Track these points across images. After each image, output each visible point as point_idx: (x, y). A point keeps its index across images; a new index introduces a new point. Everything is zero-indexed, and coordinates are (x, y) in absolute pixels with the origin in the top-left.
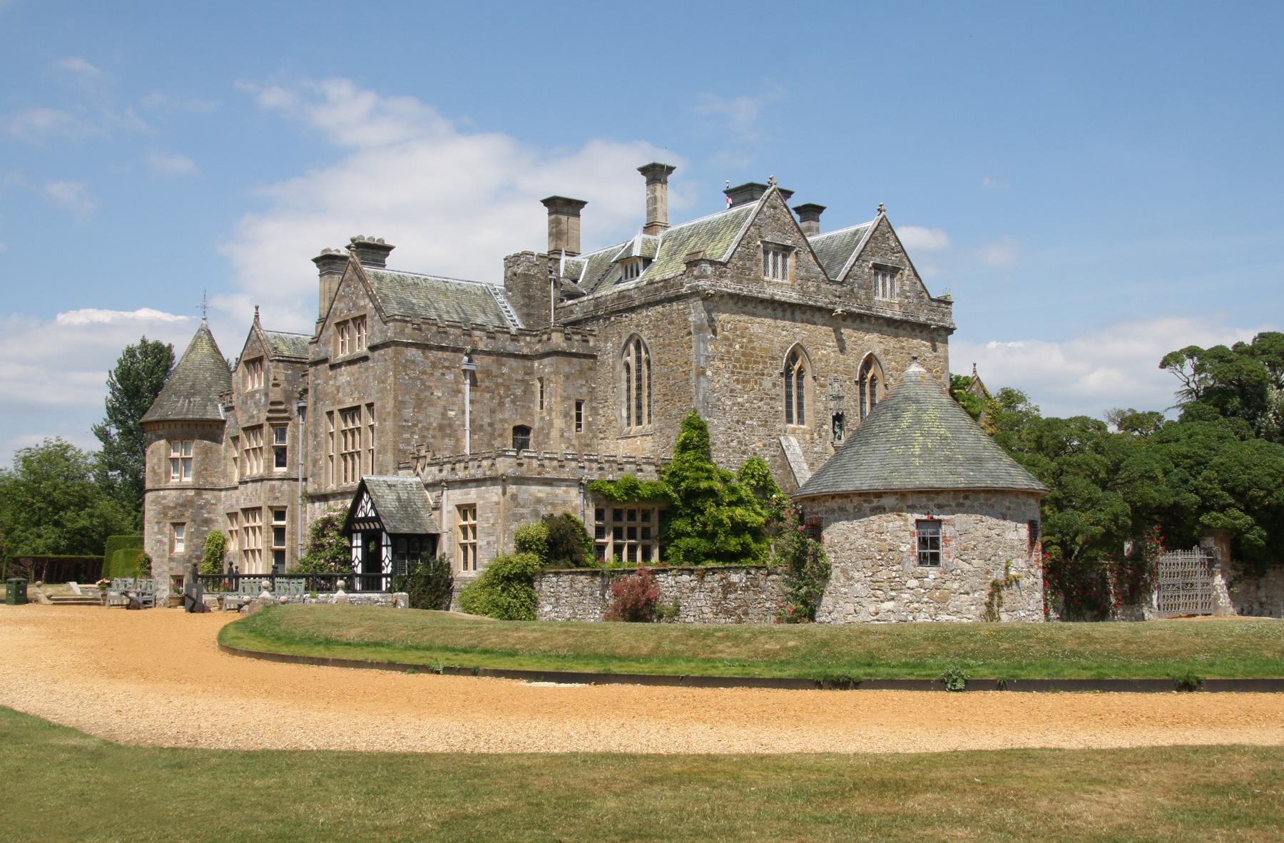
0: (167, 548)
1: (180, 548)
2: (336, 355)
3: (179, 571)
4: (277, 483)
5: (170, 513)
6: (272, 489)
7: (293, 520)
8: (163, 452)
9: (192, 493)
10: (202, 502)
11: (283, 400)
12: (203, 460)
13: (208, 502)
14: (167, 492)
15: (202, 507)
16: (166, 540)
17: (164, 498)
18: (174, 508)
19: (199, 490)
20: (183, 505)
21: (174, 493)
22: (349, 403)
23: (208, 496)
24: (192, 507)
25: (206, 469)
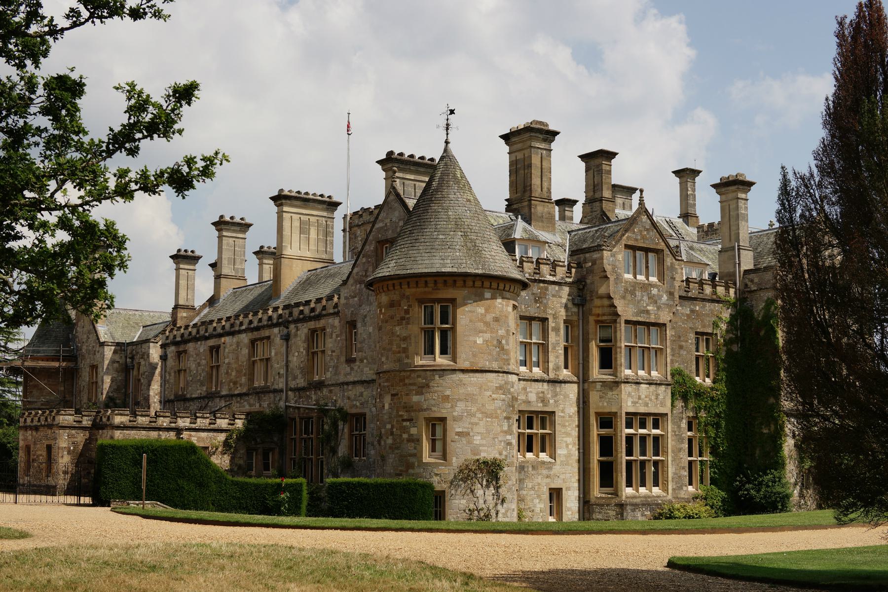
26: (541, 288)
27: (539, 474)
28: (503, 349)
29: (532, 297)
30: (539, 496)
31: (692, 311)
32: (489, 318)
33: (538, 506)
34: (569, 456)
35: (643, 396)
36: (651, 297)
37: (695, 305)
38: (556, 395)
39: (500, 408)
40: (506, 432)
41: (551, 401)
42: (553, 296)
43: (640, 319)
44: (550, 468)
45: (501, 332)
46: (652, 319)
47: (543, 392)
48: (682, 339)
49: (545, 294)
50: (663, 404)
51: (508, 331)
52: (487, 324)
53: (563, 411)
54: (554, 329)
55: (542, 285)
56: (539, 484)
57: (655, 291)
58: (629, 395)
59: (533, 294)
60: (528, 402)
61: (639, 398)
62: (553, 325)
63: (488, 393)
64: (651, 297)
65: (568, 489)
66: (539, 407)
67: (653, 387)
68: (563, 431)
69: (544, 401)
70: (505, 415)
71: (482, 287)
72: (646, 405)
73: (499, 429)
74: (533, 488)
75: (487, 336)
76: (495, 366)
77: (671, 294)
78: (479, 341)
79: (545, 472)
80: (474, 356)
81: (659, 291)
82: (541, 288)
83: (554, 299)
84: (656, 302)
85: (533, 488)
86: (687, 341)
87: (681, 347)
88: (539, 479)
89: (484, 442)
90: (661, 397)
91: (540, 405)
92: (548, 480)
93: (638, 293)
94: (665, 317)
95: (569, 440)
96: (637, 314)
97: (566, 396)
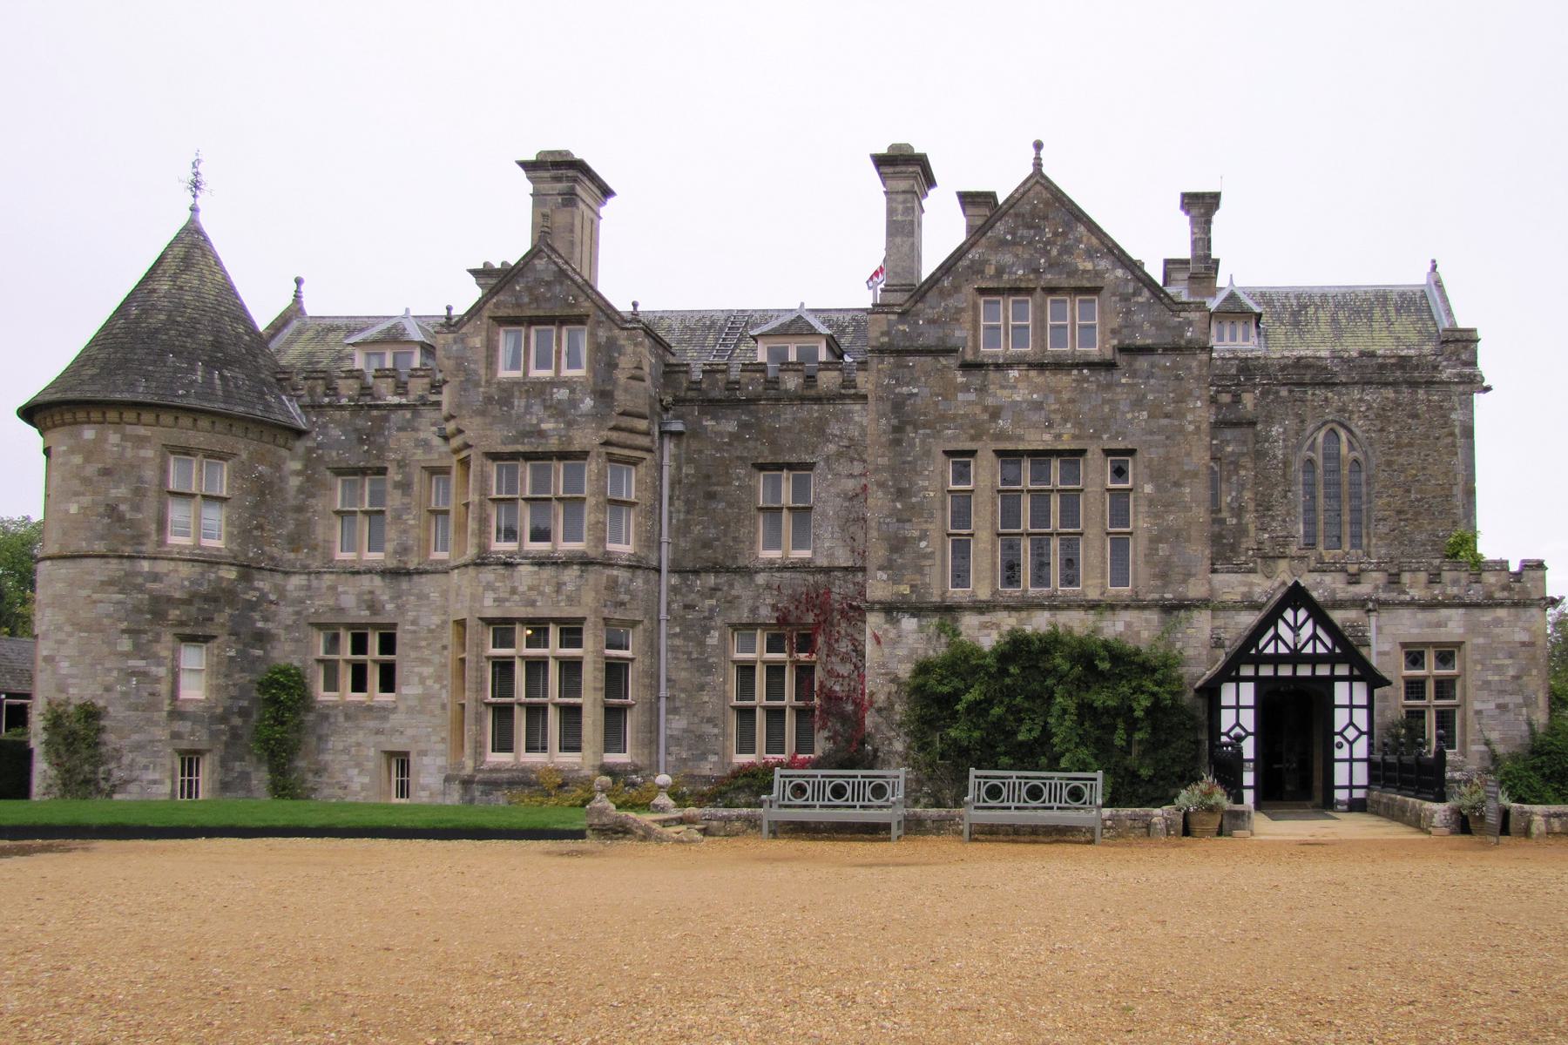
3: (198, 737)
5: (174, 614)
6: (613, 585)
7: (653, 649)
8: (150, 474)
10: (252, 596)
11: (646, 410)
12: (256, 506)
13: (263, 597)
14: (163, 567)
15: (252, 606)
17: (156, 577)
18: (188, 602)
19: (248, 570)
20: (208, 598)
21: (185, 570)
23: (263, 583)
25: (260, 527)
26: (373, 419)
27: (359, 728)
28: (121, 518)
29: (354, 436)
30: (358, 765)
32: (90, 470)
33: (356, 779)
34: (425, 698)
35: (521, 589)
38: (400, 597)
39: (108, 616)
40: (127, 655)
41: (389, 607)
42: (400, 429)
43: (520, 448)
44: (385, 718)
45: (122, 491)
46: (553, 444)
47: (371, 592)
48: (714, 480)
49: (382, 428)
51: (139, 492)
52: (86, 481)
53: (414, 623)
54: (397, 485)
55: (375, 413)
56: (359, 744)
58: (489, 587)
59: (356, 430)
61: (514, 591)
62: (398, 478)
63: (84, 593)
65: (423, 753)
66: (364, 615)
67: (548, 572)
68: (413, 655)
69: (373, 607)
70: (124, 625)
71: (75, 423)
72: (533, 603)
73: (105, 649)
74: (346, 750)
75: (87, 500)
76: (100, 547)
77: (604, 396)
78: (74, 509)
79: (372, 724)
80: (65, 534)
81: (572, 391)
82: (373, 419)
83: (401, 434)
86: (729, 483)
87: (711, 496)
88: (360, 736)
89: (74, 671)
90: (570, 587)
91: (367, 613)
92: (382, 738)
93: (519, 403)
94: (586, 437)
95: (427, 671)
96: (515, 440)
97: (422, 597)
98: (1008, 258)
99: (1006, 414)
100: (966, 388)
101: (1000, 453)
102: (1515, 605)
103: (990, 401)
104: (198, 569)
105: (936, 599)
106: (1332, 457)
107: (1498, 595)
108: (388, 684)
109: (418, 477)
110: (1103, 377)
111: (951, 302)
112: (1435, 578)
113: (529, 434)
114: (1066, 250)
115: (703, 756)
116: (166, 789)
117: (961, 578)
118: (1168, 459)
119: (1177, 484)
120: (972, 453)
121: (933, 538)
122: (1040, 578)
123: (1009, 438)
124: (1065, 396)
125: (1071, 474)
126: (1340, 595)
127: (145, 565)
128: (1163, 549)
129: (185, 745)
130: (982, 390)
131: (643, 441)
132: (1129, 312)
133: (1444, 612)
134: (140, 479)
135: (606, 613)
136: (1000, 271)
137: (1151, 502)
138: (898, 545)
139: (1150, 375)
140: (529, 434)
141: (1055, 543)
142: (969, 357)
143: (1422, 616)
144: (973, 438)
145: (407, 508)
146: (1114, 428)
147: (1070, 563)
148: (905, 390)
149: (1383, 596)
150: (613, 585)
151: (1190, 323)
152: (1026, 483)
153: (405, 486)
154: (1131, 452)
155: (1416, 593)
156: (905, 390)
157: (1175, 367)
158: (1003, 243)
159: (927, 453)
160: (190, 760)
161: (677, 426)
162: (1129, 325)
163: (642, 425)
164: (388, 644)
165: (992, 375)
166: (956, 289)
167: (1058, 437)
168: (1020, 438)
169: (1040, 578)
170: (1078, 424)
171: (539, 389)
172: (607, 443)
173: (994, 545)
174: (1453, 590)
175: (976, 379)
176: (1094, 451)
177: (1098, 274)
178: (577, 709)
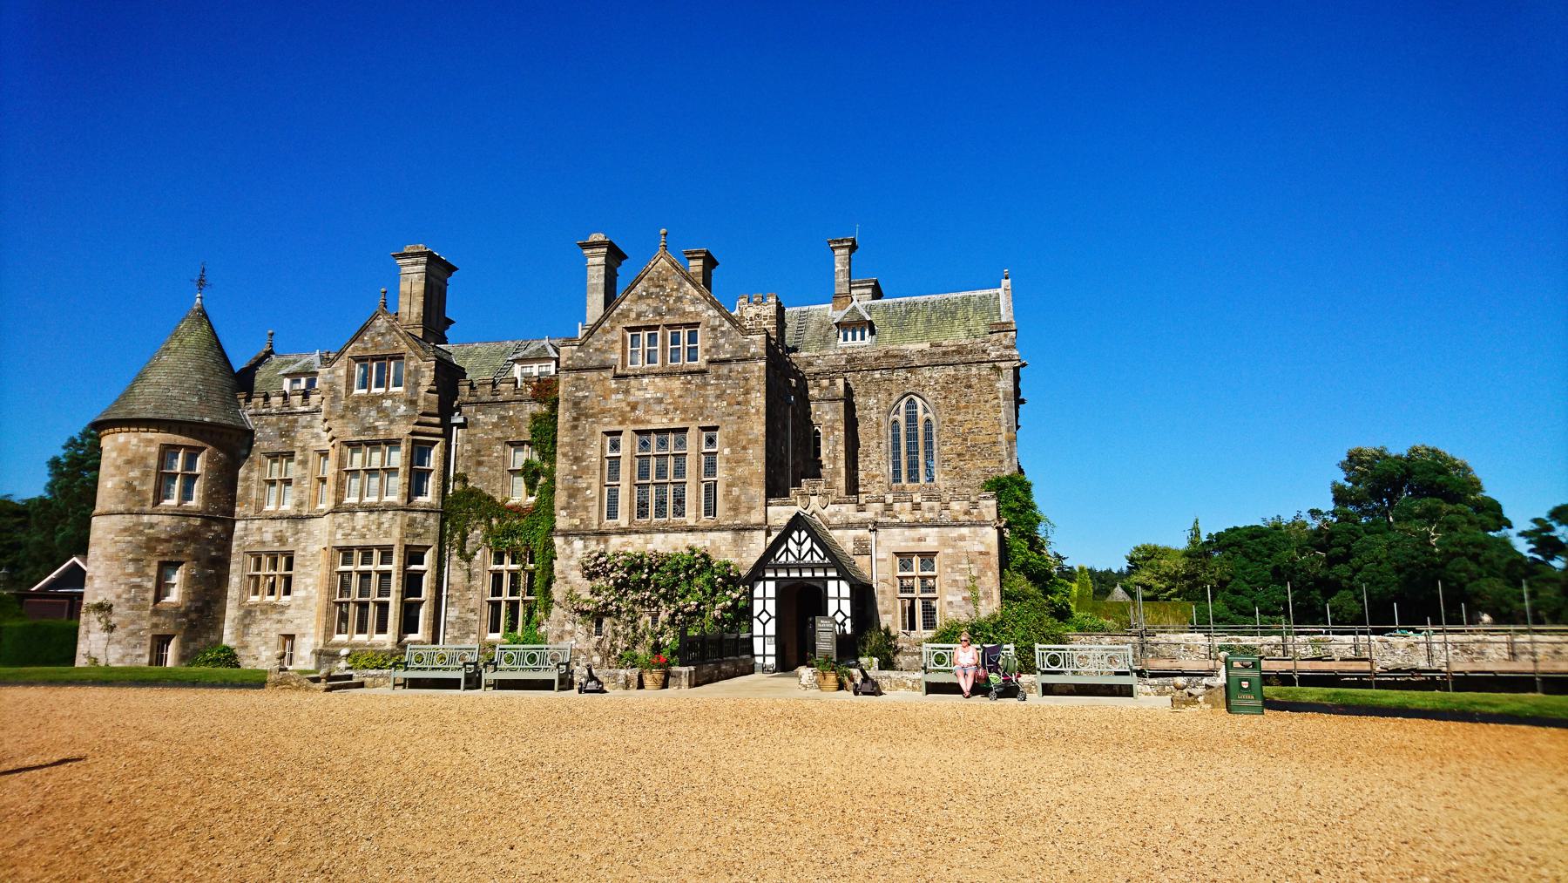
0: (151, 595)
1: (174, 596)
2: (624, 366)
4: (419, 516)
9: (198, 522)
16: (151, 585)
22: (659, 422)
24: (195, 541)
31: (502, 418)
36: (381, 410)
37: (507, 410)
46: (381, 435)
50: (387, 534)
57: (388, 403)
58: (339, 526)
60: (263, 543)
64: (381, 410)
66: (276, 547)
67: (374, 516)
69: (281, 539)
72: (364, 536)
77: (412, 403)
84: (387, 416)
85: (259, 634)
96: (359, 433)
98: (644, 307)
99: (641, 407)
100: (617, 391)
101: (638, 432)
102: (972, 525)
103: (631, 399)
104: (176, 520)
105: (595, 527)
106: (911, 418)
107: (962, 518)
108: (288, 592)
109: (312, 456)
110: (698, 380)
111: (609, 337)
112: (917, 507)
113: (368, 429)
114: (679, 299)
115: (467, 634)
116: (146, 660)
117: (613, 514)
118: (739, 431)
119: (744, 448)
120: (620, 433)
121: (592, 486)
122: (661, 512)
123: (642, 422)
124: (677, 393)
125: (681, 443)
126: (852, 520)
127: (146, 518)
128: (736, 491)
129: (159, 632)
130: (627, 392)
131: (439, 430)
132: (715, 337)
133: (923, 531)
134: (146, 466)
135: (407, 541)
136: (639, 315)
137: (728, 461)
138: (573, 493)
139: (728, 378)
140: (368, 429)
141: (652, 489)
142: (619, 371)
143: (907, 532)
144: (621, 423)
145: (304, 477)
146: (706, 412)
147: (679, 501)
148: (581, 394)
149: (880, 520)
150: (413, 520)
151: (754, 342)
152: (654, 450)
153: (304, 463)
154: (716, 428)
155: (906, 517)
156: (581, 394)
157: (744, 371)
158: (640, 297)
159: (593, 433)
160: (160, 642)
161: (460, 420)
162: (716, 346)
163: (437, 420)
164: (289, 566)
165: (633, 382)
166: (613, 328)
167: (672, 420)
168: (649, 422)
169: (661, 512)
170: (685, 411)
171: (374, 401)
172: (413, 433)
173: (631, 491)
174: (929, 515)
175: (623, 384)
176: (693, 428)
177: (698, 314)
178: (386, 604)
